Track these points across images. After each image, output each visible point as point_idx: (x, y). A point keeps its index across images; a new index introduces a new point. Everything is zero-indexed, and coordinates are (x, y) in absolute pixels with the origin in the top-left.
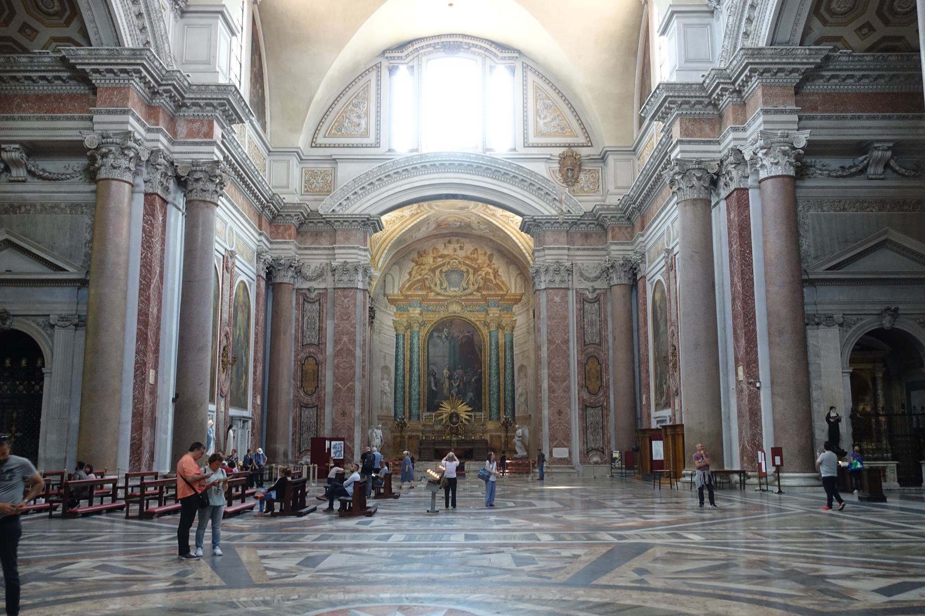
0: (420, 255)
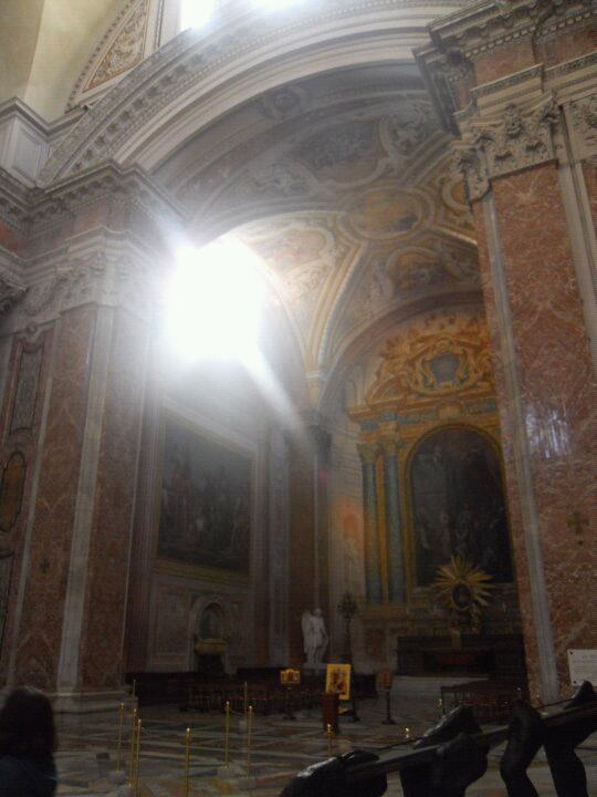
0: (391, 344)
